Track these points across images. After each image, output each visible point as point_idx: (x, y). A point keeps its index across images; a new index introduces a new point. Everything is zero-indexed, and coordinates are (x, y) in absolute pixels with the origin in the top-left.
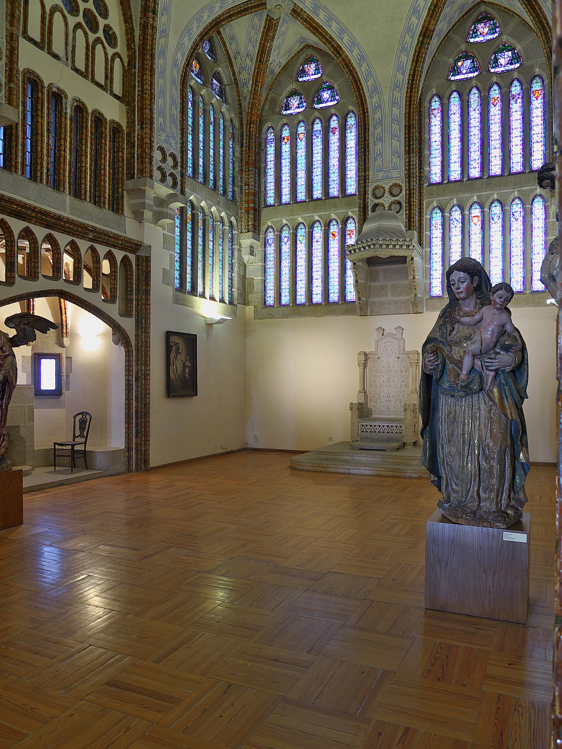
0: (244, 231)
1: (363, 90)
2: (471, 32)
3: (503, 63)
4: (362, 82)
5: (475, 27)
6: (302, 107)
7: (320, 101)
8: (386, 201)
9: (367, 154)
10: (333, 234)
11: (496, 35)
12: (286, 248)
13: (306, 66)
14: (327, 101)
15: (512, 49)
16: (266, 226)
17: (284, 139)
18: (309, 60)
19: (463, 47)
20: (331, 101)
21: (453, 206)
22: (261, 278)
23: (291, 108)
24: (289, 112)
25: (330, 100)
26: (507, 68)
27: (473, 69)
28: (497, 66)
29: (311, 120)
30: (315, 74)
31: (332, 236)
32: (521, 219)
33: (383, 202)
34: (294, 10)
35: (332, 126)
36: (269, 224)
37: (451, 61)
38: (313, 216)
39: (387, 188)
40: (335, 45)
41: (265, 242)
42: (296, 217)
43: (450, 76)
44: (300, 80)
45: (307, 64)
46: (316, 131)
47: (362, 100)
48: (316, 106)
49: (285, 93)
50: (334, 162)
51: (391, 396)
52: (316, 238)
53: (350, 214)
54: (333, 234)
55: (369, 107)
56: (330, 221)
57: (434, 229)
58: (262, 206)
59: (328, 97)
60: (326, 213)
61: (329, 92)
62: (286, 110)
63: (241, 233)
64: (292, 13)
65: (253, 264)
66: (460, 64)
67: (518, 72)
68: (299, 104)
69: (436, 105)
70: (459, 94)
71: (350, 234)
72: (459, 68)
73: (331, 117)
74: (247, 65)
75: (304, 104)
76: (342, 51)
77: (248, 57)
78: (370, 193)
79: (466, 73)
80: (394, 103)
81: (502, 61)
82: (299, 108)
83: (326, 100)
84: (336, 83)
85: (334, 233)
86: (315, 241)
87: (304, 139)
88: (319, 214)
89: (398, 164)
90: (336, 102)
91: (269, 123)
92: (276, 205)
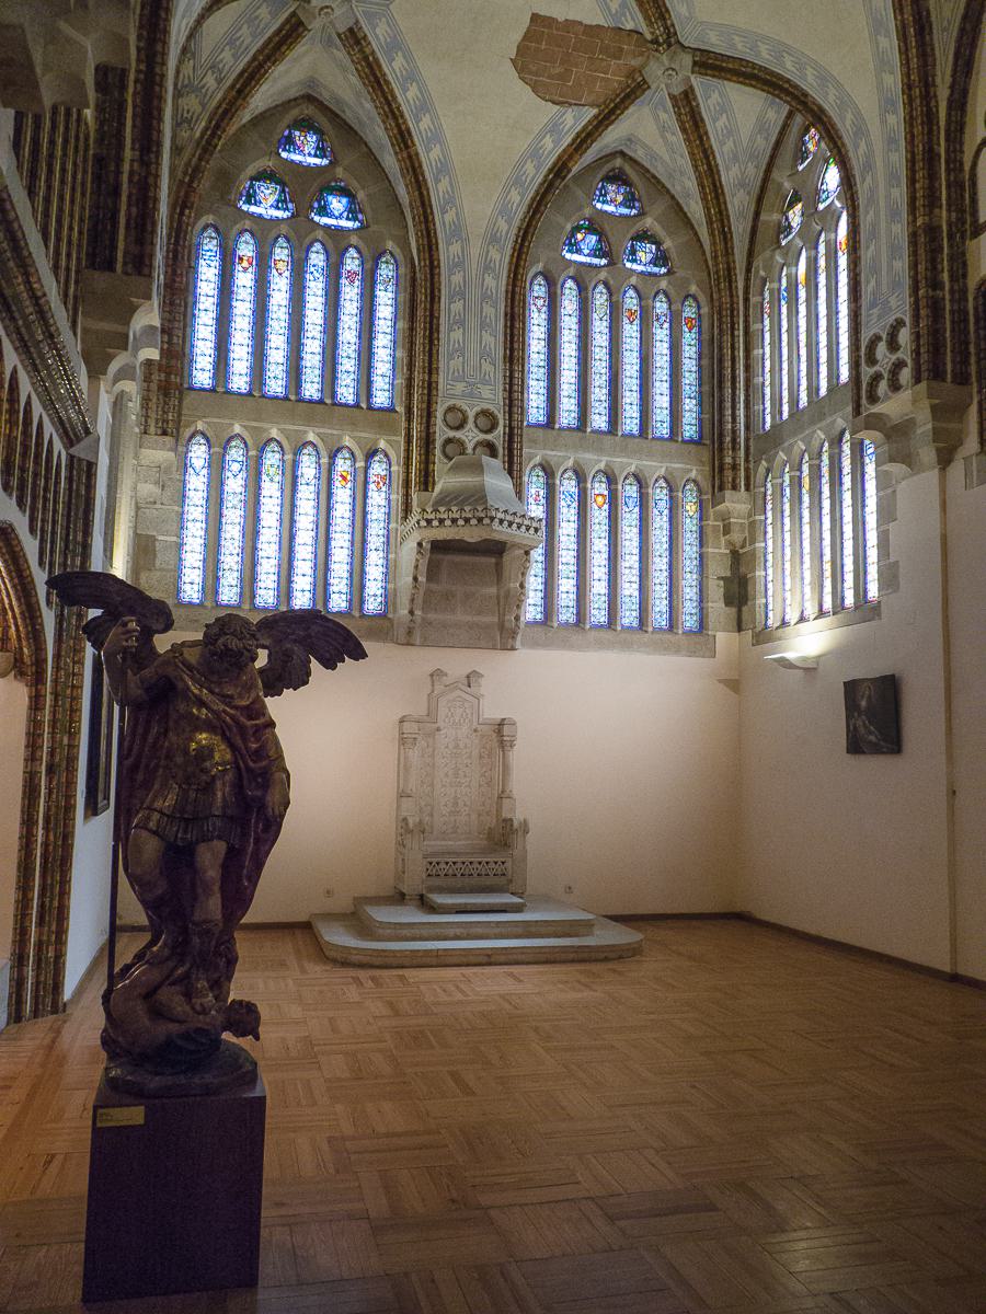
0: (152, 429)
1: (434, 225)
2: (598, 193)
3: (643, 259)
4: (435, 211)
5: (603, 187)
6: (285, 210)
7: (324, 210)
8: (470, 438)
9: (436, 342)
10: (342, 476)
11: (634, 212)
12: (235, 485)
13: (297, 133)
14: (340, 217)
15: (658, 243)
16: (192, 429)
17: (241, 259)
18: (306, 125)
19: (587, 212)
20: (348, 219)
21: (565, 470)
22: (174, 539)
23: (260, 202)
24: (253, 209)
25: (345, 214)
26: (649, 270)
27: (597, 252)
28: (634, 261)
29: (307, 241)
30: (316, 156)
31: (340, 479)
32: (666, 512)
33: (464, 438)
34: (351, 30)
35: (349, 268)
36: (200, 426)
37: (569, 227)
38: (305, 432)
39: (471, 415)
40: (403, 127)
41: (186, 465)
42: (265, 425)
43: (241, 202)
44: (284, 155)
45: (301, 131)
46: (314, 266)
47: (430, 241)
48: (317, 219)
49: (251, 170)
50: (348, 334)
51: (461, 803)
52: (306, 477)
53: (382, 444)
54: (342, 476)
55: (442, 258)
56: (339, 450)
57: (533, 502)
58: (186, 386)
59: (342, 209)
60: (335, 432)
61: (344, 200)
62: (248, 202)
63: (145, 433)
64: (348, 34)
65: (158, 506)
66: (580, 236)
67: (669, 283)
68: (278, 201)
69: (539, 290)
70: (578, 286)
71: (378, 483)
72: (577, 243)
73: (346, 250)
74: (203, 87)
75: (290, 205)
76: (412, 141)
77: (213, 73)
78: (439, 414)
79: (588, 255)
80: (487, 268)
81: (641, 255)
82: (278, 208)
83: (337, 214)
84: (363, 188)
85: (344, 474)
86: (303, 482)
87: (287, 274)
88: (317, 431)
89: (492, 375)
90: (357, 224)
91: (211, 217)
92: (219, 389)
